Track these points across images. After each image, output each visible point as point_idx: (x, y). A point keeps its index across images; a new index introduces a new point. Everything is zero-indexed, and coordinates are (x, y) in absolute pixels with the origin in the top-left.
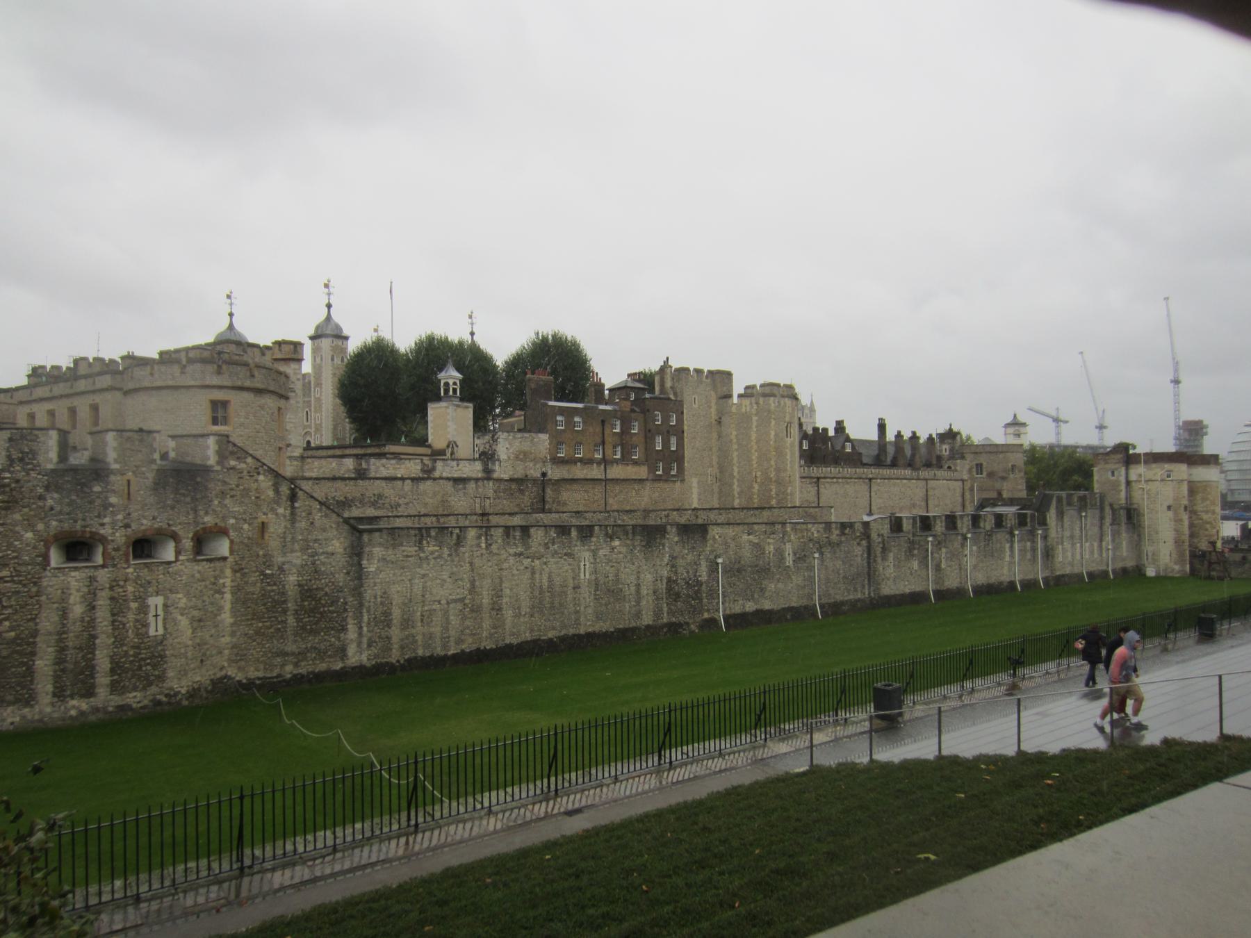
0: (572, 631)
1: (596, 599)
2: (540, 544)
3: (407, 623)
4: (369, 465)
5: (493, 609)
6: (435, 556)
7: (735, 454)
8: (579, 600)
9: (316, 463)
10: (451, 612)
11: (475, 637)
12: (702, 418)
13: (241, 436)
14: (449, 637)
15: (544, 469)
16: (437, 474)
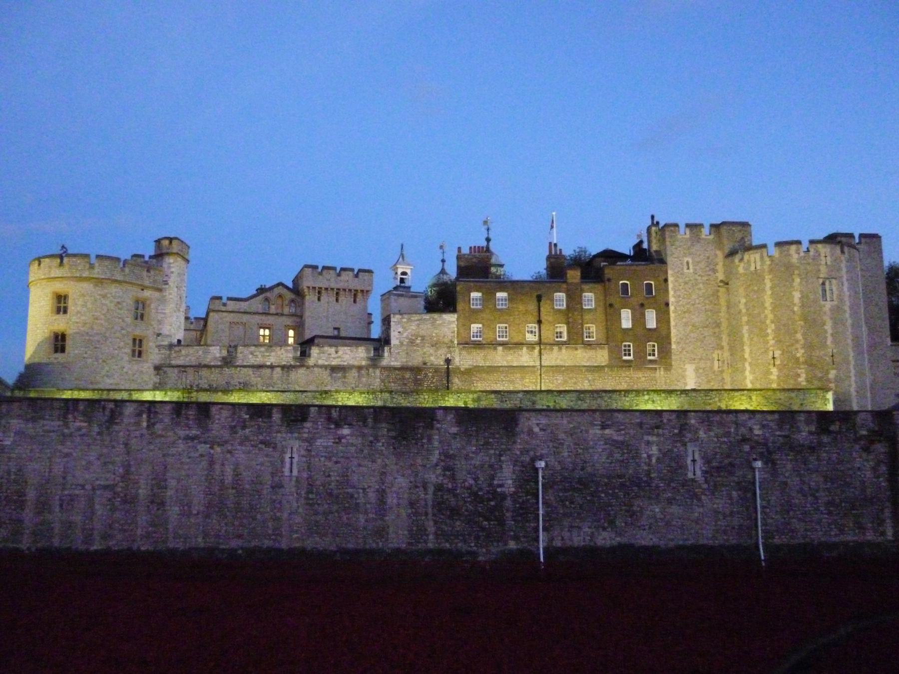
0: (267, 543)
1: (307, 504)
2: (224, 427)
3: (43, 506)
4: (236, 353)
5: (152, 502)
6: (80, 433)
7: (746, 328)
8: (280, 503)
9: (183, 352)
10: (97, 500)
11: (127, 534)
12: (701, 285)
13: (77, 323)
14: (93, 529)
15: (449, 356)
16: (311, 361)
